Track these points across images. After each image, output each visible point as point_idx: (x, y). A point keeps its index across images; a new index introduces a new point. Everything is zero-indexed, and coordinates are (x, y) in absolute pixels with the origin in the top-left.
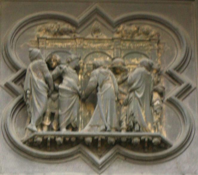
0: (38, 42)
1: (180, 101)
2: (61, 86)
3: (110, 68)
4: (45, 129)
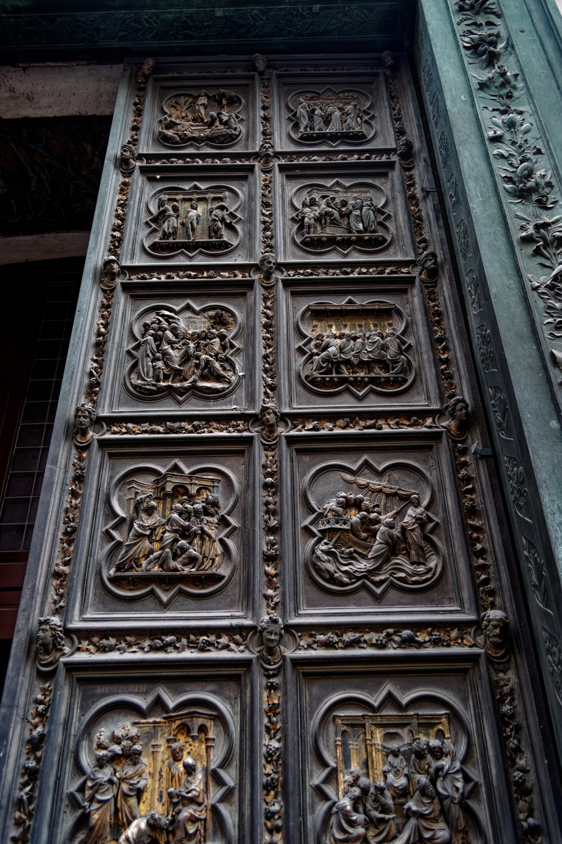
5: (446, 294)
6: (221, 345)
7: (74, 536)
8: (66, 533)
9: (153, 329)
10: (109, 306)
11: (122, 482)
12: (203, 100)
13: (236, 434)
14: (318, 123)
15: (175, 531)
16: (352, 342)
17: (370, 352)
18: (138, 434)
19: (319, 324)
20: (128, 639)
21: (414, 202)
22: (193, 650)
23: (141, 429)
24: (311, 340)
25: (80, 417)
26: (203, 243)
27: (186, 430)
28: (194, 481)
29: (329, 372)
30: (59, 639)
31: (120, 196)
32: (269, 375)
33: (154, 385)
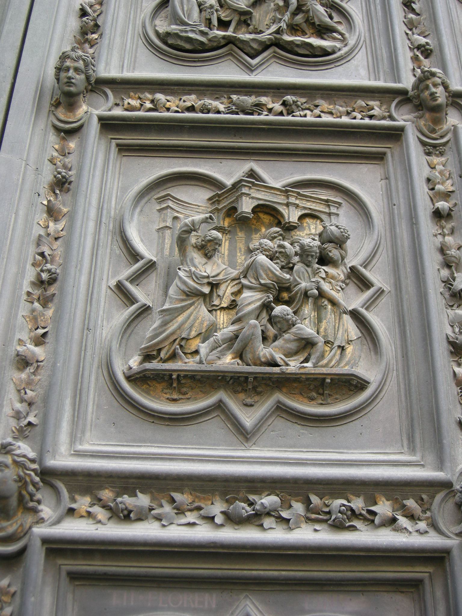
7: (52, 290)
8: (40, 283)
11: (146, 199)
13: (367, 121)
15: (265, 288)
18: (177, 112)
20: (177, 496)
22: (317, 527)
23: (182, 103)
25: (68, 69)
28: (292, 200)
30: (31, 488)
33: (203, 33)
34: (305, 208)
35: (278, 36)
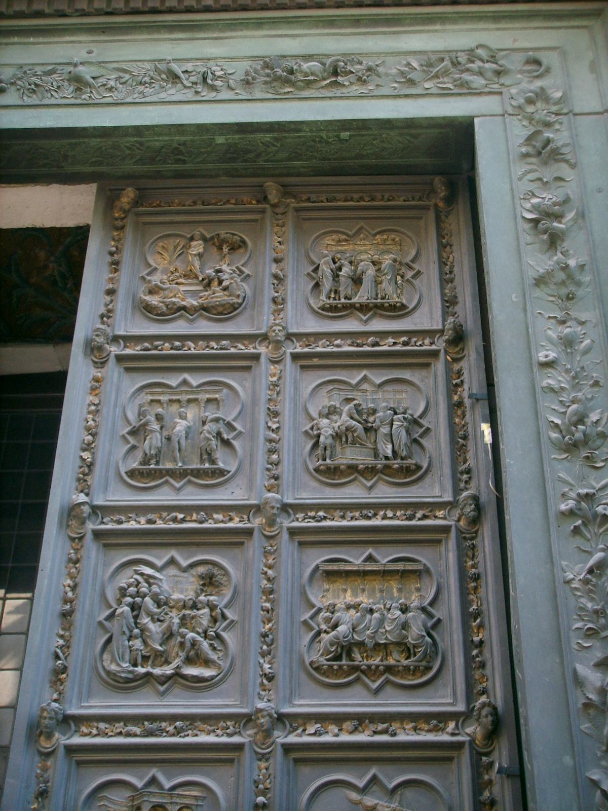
0: (327, 247)
1: (413, 281)
2: (340, 273)
3: (371, 262)
4: (332, 299)
5: (487, 549)
6: (211, 616)
9: (130, 596)
10: (77, 561)
12: (197, 247)
14: (345, 287)
16: (368, 616)
17: (389, 632)
18: (112, 736)
19: (331, 586)
21: (459, 412)
24: (320, 610)
26: (192, 470)
27: (167, 732)
29: (338, 658)
31: (91, 398)
32: (267, 659)
34: (182, 804)
35: (178, 670)
